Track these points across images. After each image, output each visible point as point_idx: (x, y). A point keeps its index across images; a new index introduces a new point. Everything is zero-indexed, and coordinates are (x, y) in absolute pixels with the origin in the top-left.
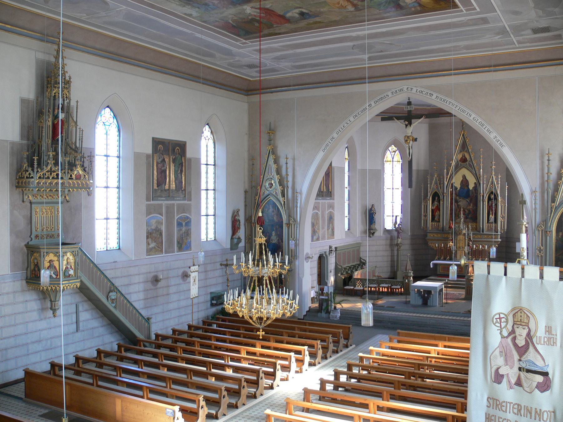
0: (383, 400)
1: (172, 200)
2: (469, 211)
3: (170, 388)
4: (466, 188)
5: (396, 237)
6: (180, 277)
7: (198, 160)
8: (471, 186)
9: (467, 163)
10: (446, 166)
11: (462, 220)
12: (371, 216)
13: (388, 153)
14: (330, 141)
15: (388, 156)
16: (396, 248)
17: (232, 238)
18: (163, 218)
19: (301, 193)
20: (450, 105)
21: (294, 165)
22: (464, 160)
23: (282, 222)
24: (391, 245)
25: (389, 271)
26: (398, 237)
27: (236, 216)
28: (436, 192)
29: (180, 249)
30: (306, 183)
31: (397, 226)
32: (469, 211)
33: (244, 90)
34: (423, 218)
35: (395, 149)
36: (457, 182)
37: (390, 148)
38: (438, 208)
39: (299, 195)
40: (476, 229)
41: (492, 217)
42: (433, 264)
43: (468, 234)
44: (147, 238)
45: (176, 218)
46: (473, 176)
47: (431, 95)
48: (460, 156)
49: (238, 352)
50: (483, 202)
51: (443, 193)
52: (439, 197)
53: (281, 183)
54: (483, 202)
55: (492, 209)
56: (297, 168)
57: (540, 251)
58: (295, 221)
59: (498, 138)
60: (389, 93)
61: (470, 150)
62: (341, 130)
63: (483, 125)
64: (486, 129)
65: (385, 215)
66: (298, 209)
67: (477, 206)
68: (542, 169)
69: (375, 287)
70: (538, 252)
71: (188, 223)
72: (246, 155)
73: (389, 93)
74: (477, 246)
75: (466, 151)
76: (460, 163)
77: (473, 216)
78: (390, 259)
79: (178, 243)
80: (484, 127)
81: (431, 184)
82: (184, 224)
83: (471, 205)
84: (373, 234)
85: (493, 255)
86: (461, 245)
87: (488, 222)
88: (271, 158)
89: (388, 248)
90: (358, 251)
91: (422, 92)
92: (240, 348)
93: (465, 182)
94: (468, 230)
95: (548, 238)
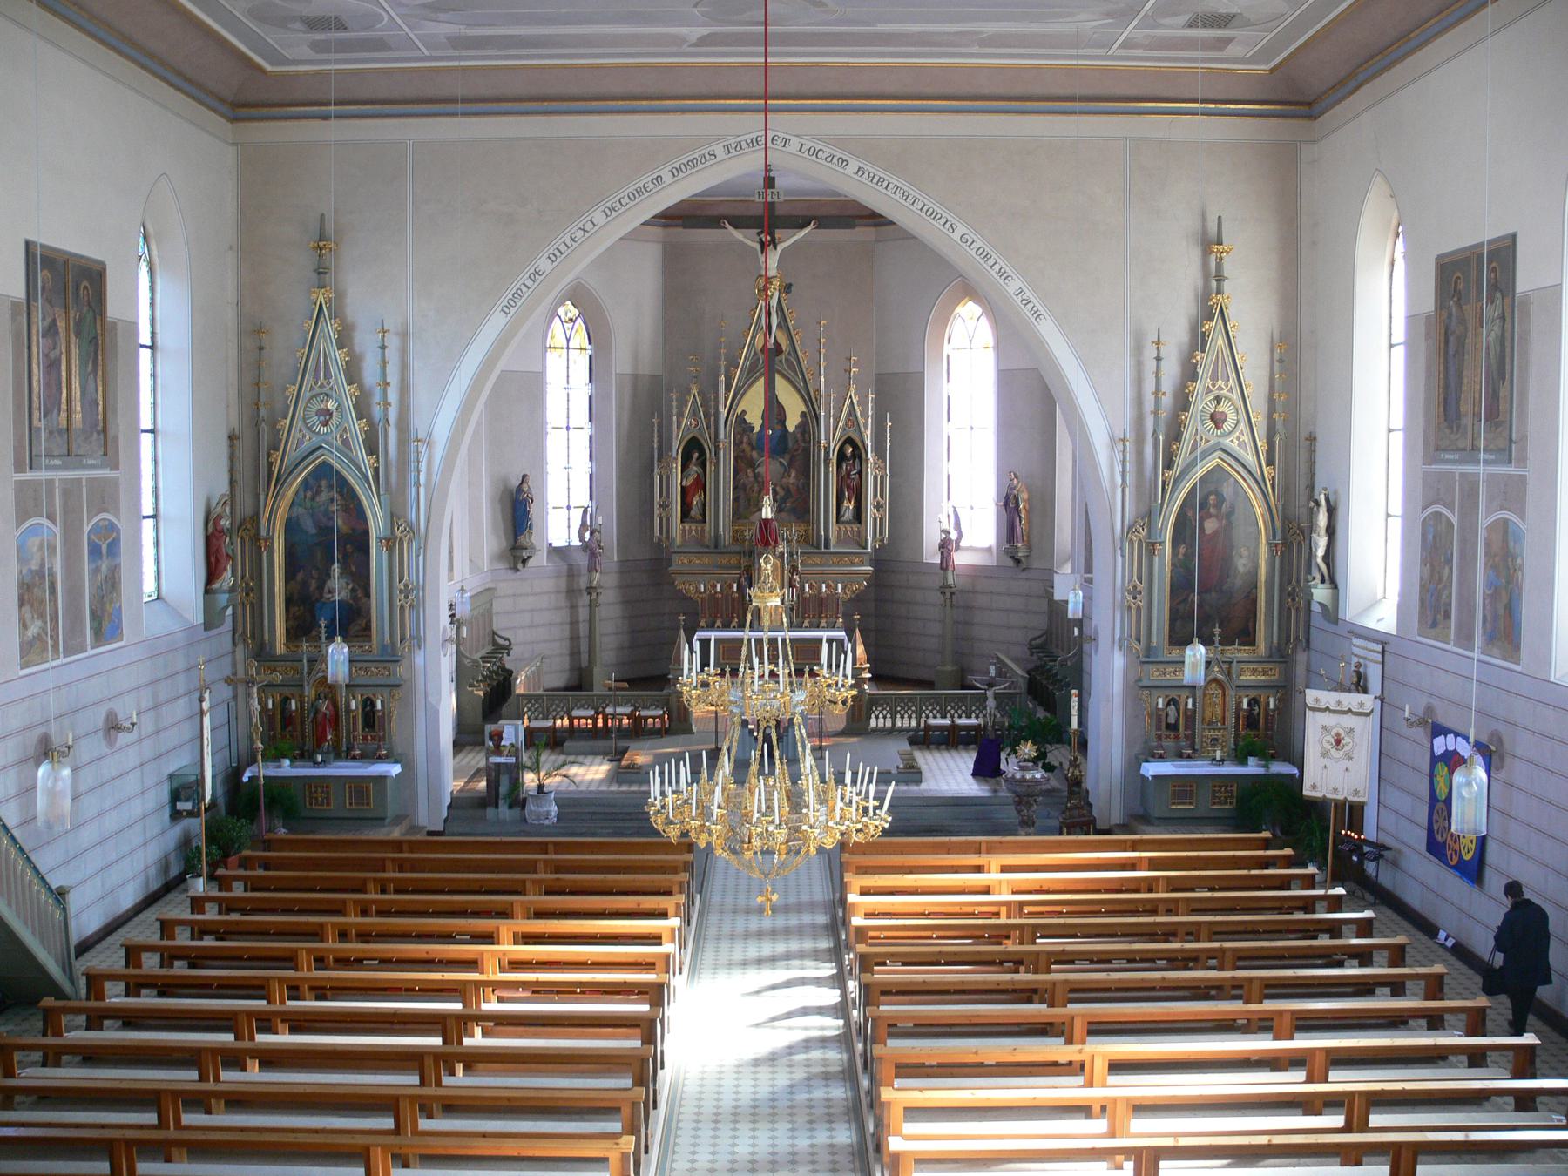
0: (1070, 1042)
1: (75, 468)
2: (787, 490)
3: (416, 1132)
4: (778, 427)
5: (584, 570)
6: (101, 734)
7: (133, 327)
8: (792, 423)
9: (783, 357)
10: (723, 363)
12: (517, 510)
14: (529, 283)
15: (557, 333)
16: (585, 599)
17: (207, 591)
18: (57, 530)
19: (429, 442)
20: (898, 197)
21: (403, 352)
23: (366, 533)
24: (571, 592)
25: (567, 666)
26: (592, 569)
27: (220, 517)
29: (100, 636)
30: (441, 411)
31: (587, 536)
32: (787, 490)
33: (222, 100)
34: (656, 512)
37: (561, 311)
38: (700, 484)
39: (423, 448)
41: (849, 506)
43: (791, 554)
44: (21, 605)
45: (87, 529)
46: (797, 396)
47: (844, 162)
49: (472, 964)
51: (716, 441)
52: (702, 453)
53: (362, 410)
55: (851, 488)
56: (415, 364)
57: (1135, 593)
58: (411, 529)
59: (1028, 294)
60: (719, 149)
61: (791, 324)
62: (563, 248)
63: (987, 257)
64: (997, 268)
65: (550, 507)
66: (422, 490)
68: (1139, 382)
69: (661, 717)
70: (1130, 598)
71: (114, 547)
72: (230, 316)
73: (719, 149)
74: (811, 587)
77: (798, 505)
78: (567, 634)
79: (93, 613)
80: (991, 262)
81: (680, 415)
82: (104, 548)
83: (793, 473)
84: (524, 561)
85: (1075, 612)
88: (330, 327)
89: (563, 602)
90: (488, 614)
91: (816, 153)
92: (482, 953)
93: (774, 411)
95: (1156, 559)
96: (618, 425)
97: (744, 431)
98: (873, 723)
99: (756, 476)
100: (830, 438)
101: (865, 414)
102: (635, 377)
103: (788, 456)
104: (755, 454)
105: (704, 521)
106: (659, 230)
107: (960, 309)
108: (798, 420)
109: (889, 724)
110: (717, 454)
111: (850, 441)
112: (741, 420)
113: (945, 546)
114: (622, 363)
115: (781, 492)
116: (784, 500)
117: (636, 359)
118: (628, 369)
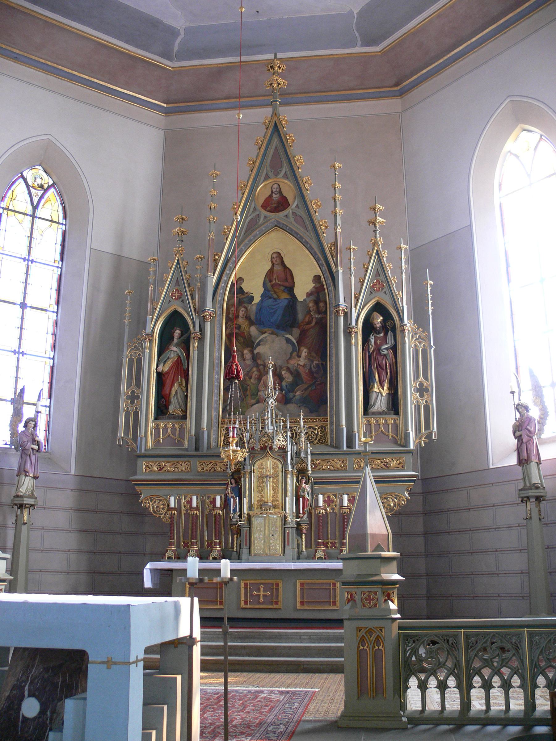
2: (296, 375)
4: (285, 296)
8: (303, 288)
9: (289, 211)
13: (20, 188)
15: (19, 197)
26: (22, 471)
28: (175, 315)
31: (21, 428)
32: (296, 375)
34: (123, 405)
35: (47, 181)
36: (251, 271)
38: (181, 369)
40: (327, 439)
41: (381, 393)
42: (153, 571)
48: (263, 190)
50: (348, 334)
51: (201, 311)
52: (185, 329)
54: (348, 334)
55: (383, 366)
67: (323, 356)
74: (328, 501)
75: (286, 176)
76: (264, 213)
77: (311, 394)
83: (304, 352)
86: (269, 495)
87: (366, 412)
93: (280, 277)
94: (295, 436)
96: (90, 308)
98: (413, 700)
99: (255, 358)
100: (353, 304)
102: (119, 260)
103: (296, 332)
104: (253, 330)
105: (184, 417)
106: (158, 117)
107: (510, 145)
108: (310, 286)
109: (453, 703)
110: (202, 330)
112: (238, 290)
113: (523, 431)
114: (101, 236)
115: (288, 378)
117: (120, 237)
118: (108, 247)
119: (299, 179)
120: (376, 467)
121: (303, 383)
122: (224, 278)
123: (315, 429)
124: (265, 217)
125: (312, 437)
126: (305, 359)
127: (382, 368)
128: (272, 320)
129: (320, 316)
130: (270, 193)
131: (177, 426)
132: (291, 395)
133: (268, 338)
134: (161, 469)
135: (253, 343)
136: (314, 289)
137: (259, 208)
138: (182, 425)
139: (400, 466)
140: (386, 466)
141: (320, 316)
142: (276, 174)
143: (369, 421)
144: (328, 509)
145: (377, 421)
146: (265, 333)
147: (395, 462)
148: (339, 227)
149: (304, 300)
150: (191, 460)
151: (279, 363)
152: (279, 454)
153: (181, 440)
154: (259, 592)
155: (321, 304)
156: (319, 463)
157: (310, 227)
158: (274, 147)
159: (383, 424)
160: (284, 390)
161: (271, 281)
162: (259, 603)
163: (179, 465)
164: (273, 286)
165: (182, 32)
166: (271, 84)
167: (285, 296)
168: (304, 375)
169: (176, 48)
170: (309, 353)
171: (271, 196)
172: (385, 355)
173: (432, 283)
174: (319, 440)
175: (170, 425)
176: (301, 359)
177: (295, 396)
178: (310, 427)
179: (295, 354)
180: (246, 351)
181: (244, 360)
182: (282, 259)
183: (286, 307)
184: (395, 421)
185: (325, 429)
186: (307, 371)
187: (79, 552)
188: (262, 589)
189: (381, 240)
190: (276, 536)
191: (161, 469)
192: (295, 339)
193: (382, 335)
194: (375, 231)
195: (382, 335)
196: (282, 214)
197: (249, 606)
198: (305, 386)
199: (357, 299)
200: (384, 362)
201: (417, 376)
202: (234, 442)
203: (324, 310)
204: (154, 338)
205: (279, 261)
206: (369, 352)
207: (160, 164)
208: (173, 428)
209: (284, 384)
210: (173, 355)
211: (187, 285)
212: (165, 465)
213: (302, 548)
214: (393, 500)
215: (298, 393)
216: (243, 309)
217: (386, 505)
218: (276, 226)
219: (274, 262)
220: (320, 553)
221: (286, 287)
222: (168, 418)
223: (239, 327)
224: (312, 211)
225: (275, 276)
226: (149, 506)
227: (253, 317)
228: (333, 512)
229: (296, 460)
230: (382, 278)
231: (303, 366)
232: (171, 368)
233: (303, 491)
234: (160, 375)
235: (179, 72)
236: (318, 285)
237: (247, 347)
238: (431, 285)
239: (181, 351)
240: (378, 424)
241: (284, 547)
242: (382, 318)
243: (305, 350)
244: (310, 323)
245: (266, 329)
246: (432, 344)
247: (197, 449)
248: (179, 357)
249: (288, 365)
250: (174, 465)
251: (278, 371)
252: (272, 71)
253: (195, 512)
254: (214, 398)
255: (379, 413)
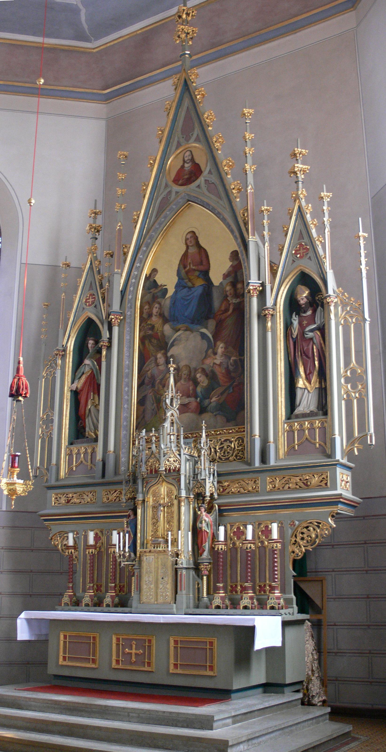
2: (212, 376)
9: (201, 180)
11: (172, 413)
22: (190, 174)
28: (90, 322)
32: (212, 376)
38: (93, 384)
42: (29, 621)
55: (307, 353)
75: (197, 140)
76: (176, 188)
83: (221, 348)
93: (195, 261)
97: (154, 298)
101: (321, 229)
102: (53, 270)
103: (212, 323)
111: (304, 279)
116: (209, 390)
117: (55, 245)
119: (210, 140)
120: (294, 486)
121: (220, 386)
122: (135, 272)
123: (231, 442)
124: (177, 193)
125: (228, 453)
126: (222, 356)
127: (307, 356)
128: (186, 314)
129: (238, 300)
130: (181, 164)
131: (89, 451)
132: (207, 402)
133: (182, 336)
134: (68, 502)
135: (167, 344)
136: (231, 269)
137: (171, 183)
138: (94, 449)
139: (323, 484)
140: (307, 485)
141: (238, 300)
142: (187, 140)
143: (291, 427)
144: (237, 543)
145: (301, 426)
146: (179, 330)
147: (317, 479)
148: (250, 187)
149: (221, 283)
150: (97, 489)
151: (193, 365)
152: (174, 477)
153: (93, 467)
154: (132, 649)
155: (239, 286)
156: (228, 485)
157: (223, 195)
158: (185, 108)
159: (309, 429)
160: (199, 397)
161: (185, 267)
162: (131, 663)
163: (85, 497)
164: (187, 273)
165: (81, 7)
166: (179, 37)
167: (200, 282)
168: (220, 377)
169: (86, 26)
170: (226, 348)
171: (183, 167)
172: (311, 339)
173: (366, 235)
174: (236, 456)
175: (83, 450)
176: (218, 357)
177: (211, 403)
178: (226, 441)
179: (210, 351)
180: (159, 355)
181: (158, 365)
182: (196, 238)
183: (202, 295)
184: (322, 423)
185: (243, 441)
186: (224, 371)
187: (13, 594)
188: (134, 646)
189: (304, 192)
190: (166, 579)
191: (68, 502)
192: (211, 333)
193: (309, 313)
194: (297, 182)
195: (309, 313)
196: (193, 185)
197: (120, 666)
198: (220, 390)
199: (274, 273)
200: (310, 347)
201: (347, 362)
202: (15, 474)
203: (242, 292)
204: (68, 352)
205: (193, 242)
206: (292, 337)
207: (102, 157)
208: (86, 453)
209: (199, 389)
210: (87, 369)
211: (99, 286)
212: (73, 497)
213: (203, 593)
214: (314, 529)
215: (214, 399)
216: (157, 305)
217: (305, 536)
218: (189, 201)
219: (189, 244)
220: (217, 600)
221: (201, 272)
222: (88, 442)
223: (152, 328)
224: (223, 174)
225: (189, 260)
226: (58, 544)
227: (166, 314)
228: (262, 546)
229: (193, 484)
230: (306, 240)
231: (220, 365)
232: (85, 383)
233: (201, 523)
234: (76, 394)
235: (107, 51)
236: (236, 263)
237: (161, 350)
238: (364, 238)
239: (93, 363)
240: (301, 430)
241: (176, 593)
242: (307, 292)
243: (221, 345)
244: (226, 310)
245: (180, 326)
246: (367, 316)
247: (103, 476)
248: (93, 372)
249: (205, 366)
250: (81, 495)
251: (192, 374)
252: (180, 21)
253: (91, 551)
254: (124, 415)
255: (304, 415)
